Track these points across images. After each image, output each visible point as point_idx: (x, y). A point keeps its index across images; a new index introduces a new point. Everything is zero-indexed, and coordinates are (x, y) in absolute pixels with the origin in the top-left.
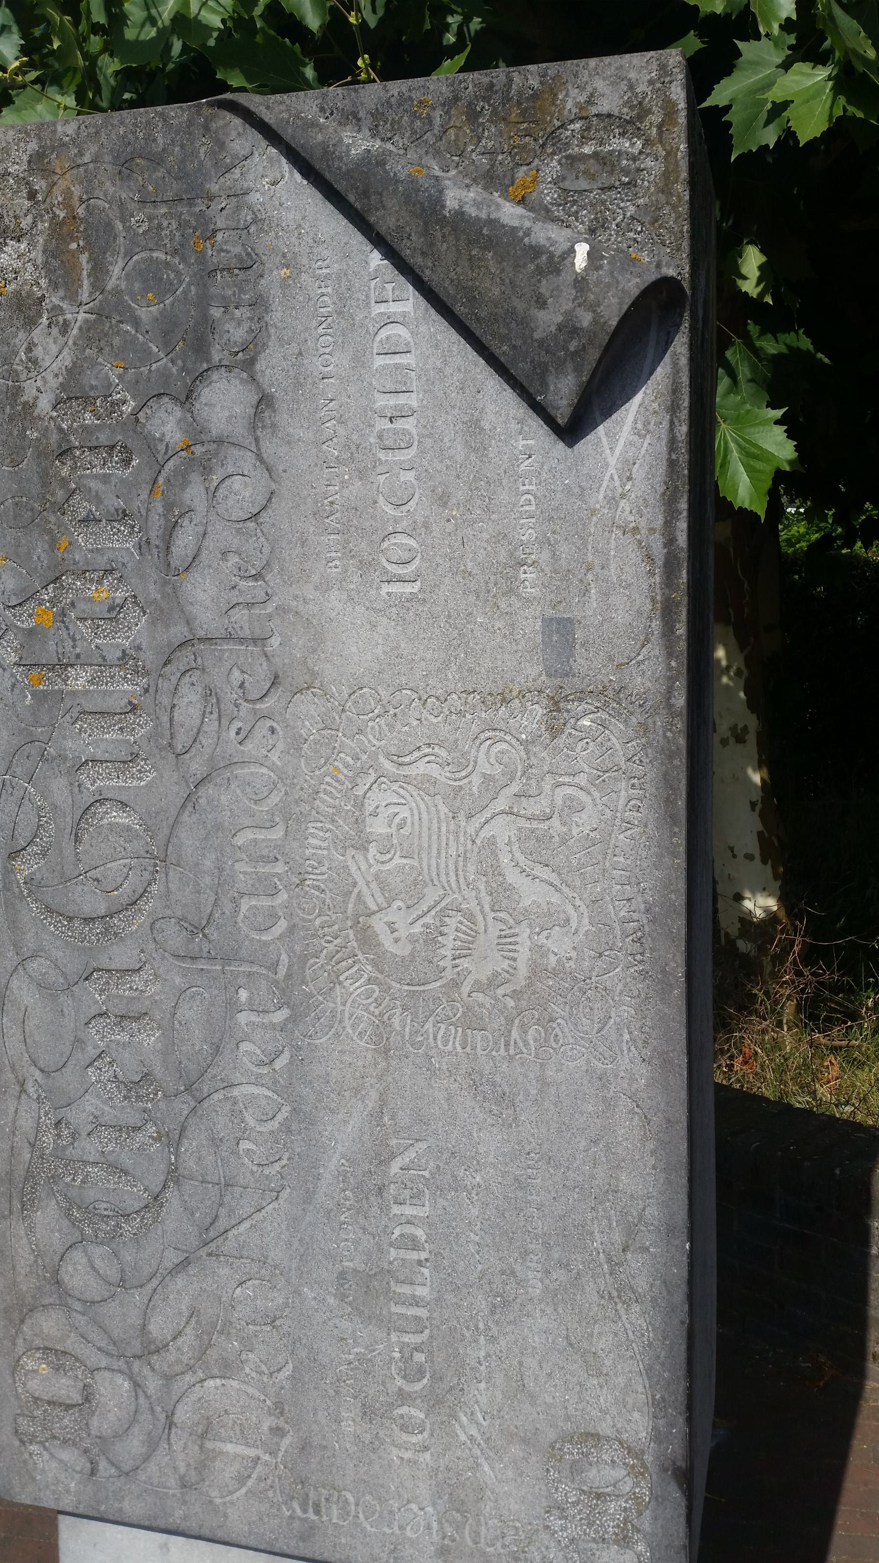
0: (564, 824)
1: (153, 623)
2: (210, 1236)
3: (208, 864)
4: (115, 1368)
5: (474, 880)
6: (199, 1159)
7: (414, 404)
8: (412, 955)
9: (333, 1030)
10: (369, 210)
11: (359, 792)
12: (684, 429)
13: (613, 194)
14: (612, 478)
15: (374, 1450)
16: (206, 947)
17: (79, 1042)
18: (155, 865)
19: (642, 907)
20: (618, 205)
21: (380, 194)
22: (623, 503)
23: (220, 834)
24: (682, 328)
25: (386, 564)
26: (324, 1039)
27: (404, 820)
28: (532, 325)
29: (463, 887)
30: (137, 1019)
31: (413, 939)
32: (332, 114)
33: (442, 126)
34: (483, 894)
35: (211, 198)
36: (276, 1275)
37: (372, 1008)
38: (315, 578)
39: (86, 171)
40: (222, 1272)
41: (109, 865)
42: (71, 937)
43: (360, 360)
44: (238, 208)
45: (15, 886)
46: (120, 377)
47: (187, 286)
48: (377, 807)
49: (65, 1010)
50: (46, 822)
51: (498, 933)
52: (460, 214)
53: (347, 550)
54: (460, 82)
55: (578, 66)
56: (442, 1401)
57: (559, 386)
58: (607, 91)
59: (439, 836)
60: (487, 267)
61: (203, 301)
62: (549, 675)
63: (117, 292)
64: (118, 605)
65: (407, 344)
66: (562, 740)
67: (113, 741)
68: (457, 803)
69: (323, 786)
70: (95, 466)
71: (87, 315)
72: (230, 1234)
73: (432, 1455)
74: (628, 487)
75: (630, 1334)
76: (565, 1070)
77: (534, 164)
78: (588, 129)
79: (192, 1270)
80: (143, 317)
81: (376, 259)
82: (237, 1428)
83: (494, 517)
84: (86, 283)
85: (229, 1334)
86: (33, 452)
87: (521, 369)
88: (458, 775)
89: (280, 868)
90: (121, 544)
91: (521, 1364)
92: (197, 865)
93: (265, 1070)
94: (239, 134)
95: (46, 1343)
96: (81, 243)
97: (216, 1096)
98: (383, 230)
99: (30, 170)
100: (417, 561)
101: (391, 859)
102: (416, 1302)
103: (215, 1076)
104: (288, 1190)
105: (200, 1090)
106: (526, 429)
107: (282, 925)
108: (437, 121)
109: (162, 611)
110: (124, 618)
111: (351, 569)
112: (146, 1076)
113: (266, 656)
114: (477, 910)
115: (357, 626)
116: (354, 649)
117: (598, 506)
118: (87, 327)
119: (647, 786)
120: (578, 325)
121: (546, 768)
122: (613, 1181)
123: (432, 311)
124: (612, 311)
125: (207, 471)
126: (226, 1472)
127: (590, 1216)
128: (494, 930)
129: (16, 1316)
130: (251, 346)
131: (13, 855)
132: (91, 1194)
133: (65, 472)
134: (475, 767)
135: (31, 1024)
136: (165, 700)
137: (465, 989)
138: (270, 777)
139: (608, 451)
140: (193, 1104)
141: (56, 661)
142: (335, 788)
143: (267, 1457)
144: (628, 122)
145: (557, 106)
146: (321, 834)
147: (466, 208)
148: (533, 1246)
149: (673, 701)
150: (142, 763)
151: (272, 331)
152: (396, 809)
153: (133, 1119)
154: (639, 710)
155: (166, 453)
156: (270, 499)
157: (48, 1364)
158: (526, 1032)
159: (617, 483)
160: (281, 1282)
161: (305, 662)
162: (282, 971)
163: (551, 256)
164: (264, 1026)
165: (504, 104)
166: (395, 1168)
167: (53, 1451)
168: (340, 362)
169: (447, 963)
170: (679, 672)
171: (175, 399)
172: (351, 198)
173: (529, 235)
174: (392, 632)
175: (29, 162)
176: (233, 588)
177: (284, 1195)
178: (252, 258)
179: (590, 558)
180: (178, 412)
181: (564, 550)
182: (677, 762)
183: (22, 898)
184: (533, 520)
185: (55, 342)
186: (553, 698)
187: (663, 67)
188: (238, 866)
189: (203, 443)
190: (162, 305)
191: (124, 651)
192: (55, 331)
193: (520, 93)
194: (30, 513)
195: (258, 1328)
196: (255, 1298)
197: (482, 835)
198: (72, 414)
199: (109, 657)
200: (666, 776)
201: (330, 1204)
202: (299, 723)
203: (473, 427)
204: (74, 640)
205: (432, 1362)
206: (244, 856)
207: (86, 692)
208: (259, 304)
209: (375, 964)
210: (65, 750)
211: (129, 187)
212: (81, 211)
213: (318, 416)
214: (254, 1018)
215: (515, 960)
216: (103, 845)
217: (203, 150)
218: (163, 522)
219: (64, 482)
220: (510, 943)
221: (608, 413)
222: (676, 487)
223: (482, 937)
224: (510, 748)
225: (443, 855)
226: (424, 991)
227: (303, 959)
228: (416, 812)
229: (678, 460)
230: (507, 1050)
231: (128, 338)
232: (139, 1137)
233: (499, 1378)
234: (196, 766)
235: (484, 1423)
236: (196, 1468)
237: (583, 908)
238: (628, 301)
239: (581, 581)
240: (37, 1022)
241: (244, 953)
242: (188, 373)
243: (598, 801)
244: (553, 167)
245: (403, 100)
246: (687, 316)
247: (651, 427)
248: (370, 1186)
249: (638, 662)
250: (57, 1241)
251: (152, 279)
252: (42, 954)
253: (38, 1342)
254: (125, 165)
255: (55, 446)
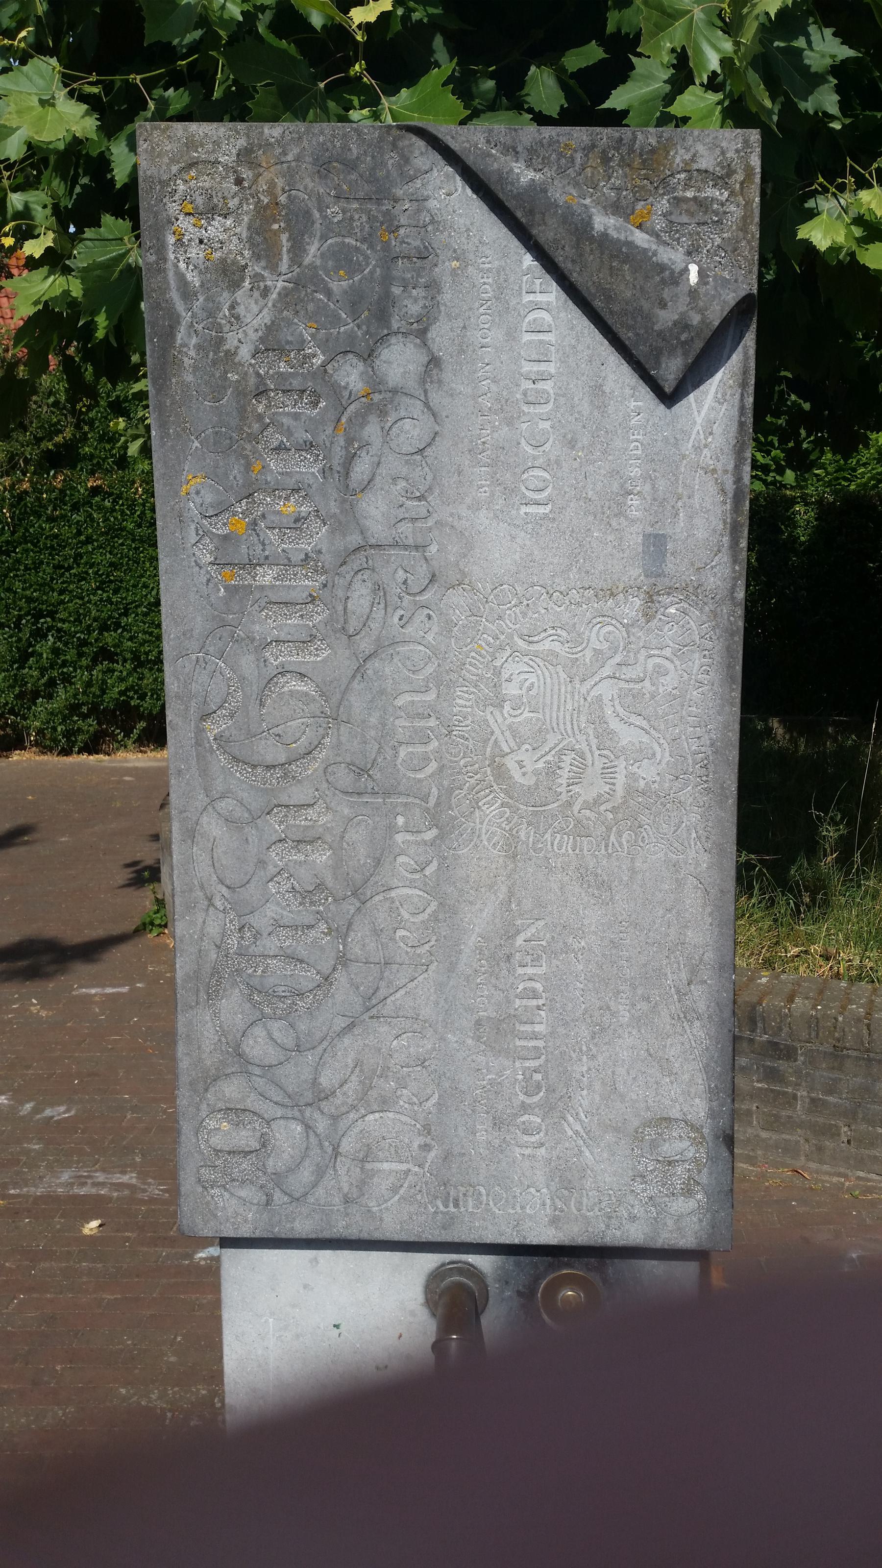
0: (653, 685)
1: (332, 532)
2: (371, 1005)
3: (373, 720)
4: (290, 1116)
5: (585, 727)
6: (364, 946)
7: (553, 371)
8: (536, 784)
9: (473, 843)
10: (532, 225)
11: (498, 663)
12: (751, 400)
13: (705, 228)
14: (698, 432)
15: (502, 1152)
16: (370, 784)
17: (262, 863)
18: (329, 723)
19: (708, 742)
20: (709, 237)
21: (544, 214)
22: (705, 451)
23: (384, 697)
24: (751, 328)
25: (525, 491)
26: (466, 850)
27: (532, 684)
28: (654, 320)
29: (577, 732)
30: (311, 842)
31: (536, 773)
32: (496, 146)
33: (582, 165)
34: (592, 737)
35: (396, 200)
36: (426, 1027)
37: (504, 825)
38: (468, 500)
39: (288, 168)
40: (382, 1030)
41: (289, 724)
42: (254, 781)
43: (512, 335)
44: (419, 211)
45: (206, 742)
46: (313, 336)
47: (372, 266)
48: (512, 675)
49: (249, 839)
50: (235, 691)
51: (602, 766)
52: (605, 235)
53: (495, 479)
54: (597, 134)
55: (685, 133)
56: (555, 1107)
57: (669, 364)
58: (706, 153)
59: (559, 695)
60: (623, 276)
61: (387, 280)
62: (646, 576)
63: (313, 267)
64: (303, 518)
65: (550, 326)
66: (654, 623)
67: (295, 626)
68: (574, 670)
69: (468, 660)
70: (287, 406)
71: (285, 284)
72: (389, 1001)
73: (547, 1149)
74: (710, 440)
75: (693, 1043)
76: (649, 861)
77: (649, 201)
78: (690, 179)
79: (356, 1031)
80: (335, 289)
81: (528, 260)
82: (392, 1150)
83: (610, 458)
84: (285, 257)
85: (387, 1076)
86: (233, 392)
87: (640, 351)
88: (575, 650)
89: (432, 722)
90: (307, 469)
91: (613, 1073)
92: (364, 722)
93: (417, 876)
94: (422, 153)
95: (228, 1105)
96: (282, 224)
97: (377, 898)
98: (542, 240)
99: (239, 161)
100: (549, 490)
101: (521, 714)
102: (535, 1036)
103: (377, 882)
104: (436, 963)
105: (364, 894)
106: (637, 394)
107: (433, 766)
108: (578, 161)
109: (340, 523)
110: (307, 528)
111: (498, 494)
112: (320, 886)
113: (426, 560)
114: (586, 749)
115: (502, 535)
116: (497, 555)
117: (687, 453)
118: (285, 294)
119: (715, 656)
120: (689, 323)
121: (641, 644)
122: (682, 937)
123: (570, 303)
124: (716, 314)
125: (383, 413)
126: (381, 1185)
127: (664, 963)
128: (599, 763)
129: (201, 1086)
130: (425, 319)
131: (205, 717)
132: (271, 981)
133: (260, 409)
134: (588, 643)
135: (219, 851)
136: (340, 593)
137: (576, 808)
138: (426, 653)
139: (696, 413)
140: (358, 905)
141: (247, 561)
142: (478, 661)
143: (416, 1169)
144: (719, 178)
145: (668, 160)
146: (466, 696)
147: (610, 231)
148: (623, 987)
149: (736, 594)
150: (319, 643)
151: (442, 308)
152: (526, 676)
153: (309, 919)
154: (711, 601)
155: (349, 398)
156: (434, 437)
157: (228, 1122)
158: (621, 836)
159: (702, 437)
160: (430, 1033)
161: (458, 565)
162: (432, 801)
163: (672, 272)
164: (418, 843)
165: (629, 154)
166: (519, 941)
167: (232, 1191)
168: (495, 336)
169: (562, 789)
170: (741, 574)
171: (358, 355)
172: (519, 214)
173: (656, 255)
174: (528, 543)
175: (238, 155)
176: (401, 506)
177: (433, 967)
178: (428, 251)
179: (680, 490)
180: (361, 366)
181: (662, 484)
182: (736, 639)
183: (212, 751)
184: (639, 461)
185: (256, 303)
186: (648, 593)
187: (746, 142)
188: (397, 722)
189: (380, 392)
190: (351, 281)
191: (306, 554)
192: (256, 294)
193: (642, 148)
194: (228, 441)
195: (411, 1069)
196: (409, 1046)
197: (592, 694)
198: (268, 362)
199: (293, 559)
200: (728, 649)
201: (469, 971)
202: (451, 612)
203: (597, 390)
204: (264, 544)
205: (547, 1079)
206: (403, 714)
207: (273, 587)
208: (433, 287)
209: (506, 792)
210: (253, 632)
211: (326, 184)
212: (283, 199)
213: (476, 376)
214: (409, 837)
215: (614, 784)
216: (284, 708)
217: (390, 162)
218: (344, 453)
219: (260, 417)
220: (611, 773)
221: (696, 386)
222: (744, 441)
223: (589, 770)
224: (615, 630)
225: (562, 709)
226: (544, 811)
227: (450, 791)
228: (541, 678)
229: (745, 422)
230: (606, 850)
231: (321, 305)
232: (313, 933)
233: (597, 1086)
234: (365, 645)
235: (586, 1121)
236: (357, 1186)
237: (666, 745)
238: (727, 309)
239: (673, 507)
240: (224, 849)
241: (402, 788)
242: (371, 336)
243: (679, 667)
244: (663, 204)
245: (552, 142)
246: (755, 319)
247: (727, 397)
248: (500, 955)
249: (712, 567)
250: (239, 1021)
251: (344, 260)
252: (230, 795)
253: (220, 1105)
254: (324, 166)
255: (253, 388)
